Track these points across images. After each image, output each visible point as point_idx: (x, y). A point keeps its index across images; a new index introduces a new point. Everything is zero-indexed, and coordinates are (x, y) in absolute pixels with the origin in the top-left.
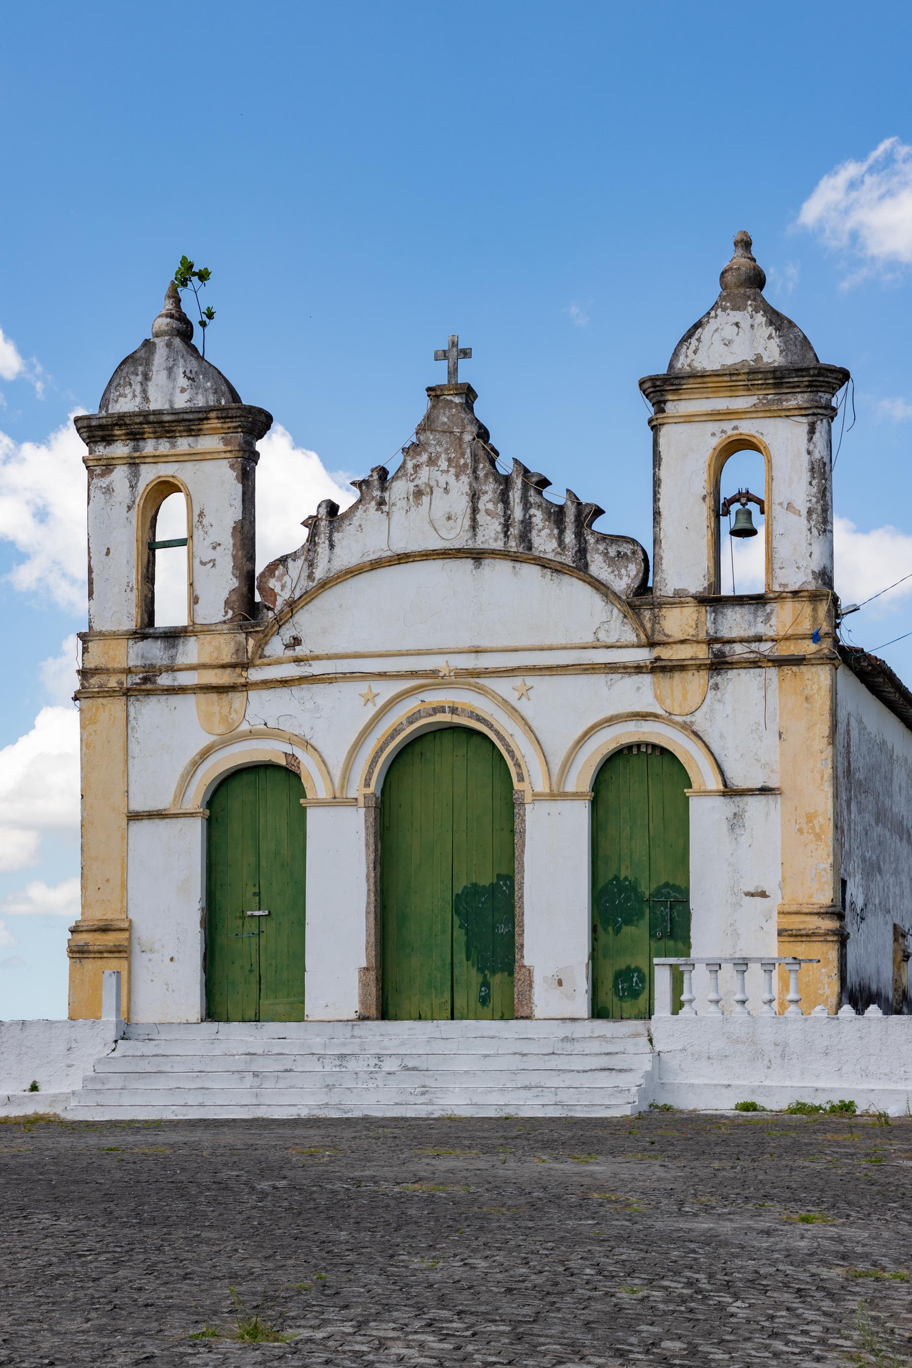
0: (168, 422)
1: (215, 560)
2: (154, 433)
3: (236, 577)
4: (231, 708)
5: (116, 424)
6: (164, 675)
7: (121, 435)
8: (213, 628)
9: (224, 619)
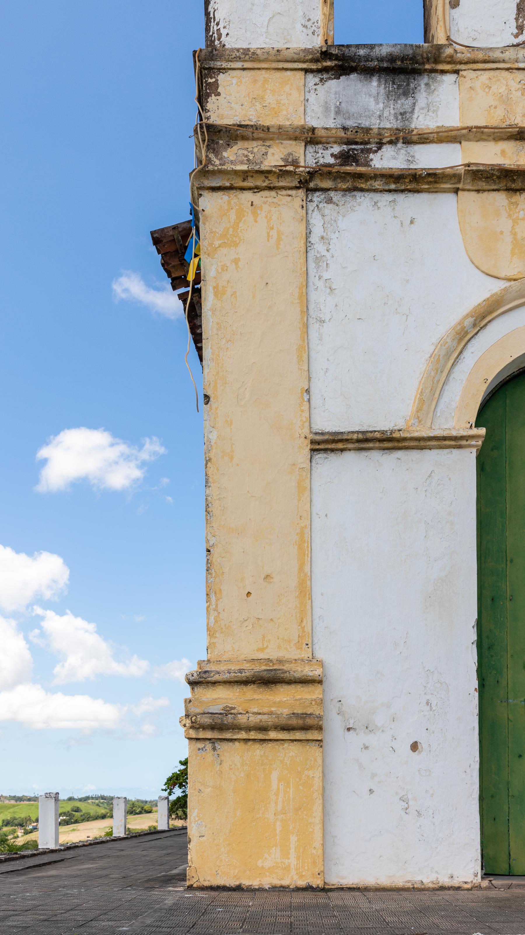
6: (388, 151)
8: (497, 55)
9: (516, 41)
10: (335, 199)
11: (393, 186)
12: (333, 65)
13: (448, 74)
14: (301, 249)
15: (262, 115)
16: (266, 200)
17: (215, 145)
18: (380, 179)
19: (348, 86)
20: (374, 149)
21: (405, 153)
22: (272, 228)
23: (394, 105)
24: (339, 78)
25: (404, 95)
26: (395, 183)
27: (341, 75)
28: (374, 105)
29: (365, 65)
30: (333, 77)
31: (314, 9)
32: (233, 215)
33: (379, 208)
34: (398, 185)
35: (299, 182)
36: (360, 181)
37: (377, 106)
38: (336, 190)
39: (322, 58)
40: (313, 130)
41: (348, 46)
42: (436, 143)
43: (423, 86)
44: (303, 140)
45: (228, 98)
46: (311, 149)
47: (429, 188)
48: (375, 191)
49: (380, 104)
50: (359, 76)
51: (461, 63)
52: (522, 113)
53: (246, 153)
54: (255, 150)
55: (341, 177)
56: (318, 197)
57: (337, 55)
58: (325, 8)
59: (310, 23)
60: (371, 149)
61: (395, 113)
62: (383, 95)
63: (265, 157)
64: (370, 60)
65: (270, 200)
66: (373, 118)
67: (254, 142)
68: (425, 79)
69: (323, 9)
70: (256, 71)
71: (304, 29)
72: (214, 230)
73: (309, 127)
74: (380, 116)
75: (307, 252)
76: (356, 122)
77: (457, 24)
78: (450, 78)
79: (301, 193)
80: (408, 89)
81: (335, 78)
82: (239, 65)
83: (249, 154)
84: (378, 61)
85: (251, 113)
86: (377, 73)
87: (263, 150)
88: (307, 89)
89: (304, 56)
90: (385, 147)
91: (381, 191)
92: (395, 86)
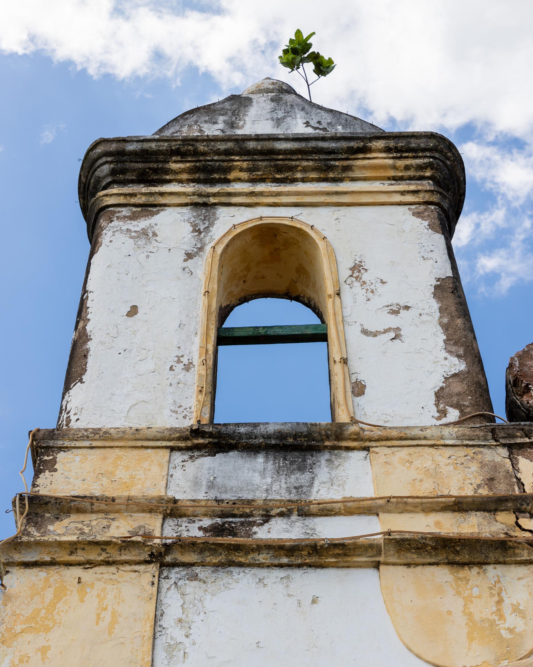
0: (285, 152)
1: (398, 329)
2: (249, 170)
3: (459, 356)
4: (500, 602)
5: (177, 152)
7: (182, 171)
10: (201, 576)
11: (285, 560)
12: (207, 442)
13: (355, 451)
14: (146, 634)
15: (108, 489)
16: (101, 576)
17: (39, 519)
18: (266, 552)
19: (226, 462)
20: (258, 521)
21: (302, 525)
22: (106, 609)
23: (286, 479)
24: (215, 455)
25: (299, 470)
26: (287, 556)
27: (218, 452)
28: (259, 479)
29: (247, 442)
30: (207, 454)
31: (187, 398)
32: (49, 595)
33: (265, 585)
34: (293, 559)
35: (149, 555)
36: (237, 554)
37: (264, 480)
38: (203, 564)
39: (192, 436)
40: (175, 501)
41: (225, 425)
42: (345, 515)
43: (323, 462)
44: (160, 513)
45: (66, 473)
46: (171, 522)
47: (337, 562)
48: (260, 566)
49: (268, 478)
50: (240, 453)
51: (370, 440)
52: (457, 486)
53: (80, 526)
54: (94, 523)
55: (210, 549)
56: (177, 573)
57: (211, 433)
58: (200, 396)
59: (182, 409)
60: (255, 522)
61: (288, 487)
62: (271, 470)
63: (106, 530)
64: (254, 437)
65: (106, 576)
66: (258, 492)
67: (93, 515)
68: (326, 455)
69: (197, 397)
70: (107, 449)
71: (174, 415)
72: (18, 612)
73: (169, 498)
74: (267, 490)
75: (154, 638)
76: (234, 496)
77: (363, 409)
78: (357, 456)
79: (153, 568)
80: (304, 464)
81: (209, 455)
82: (87, 443)
83: (85, 527)
84: (264, 438)
85: (94, 487)
86: (263, 451)
87: (105, 523)
88: (171, 465)
89: (170, 435)
90: (273, 519)
91: (268, 566)
92: (287, 462)
